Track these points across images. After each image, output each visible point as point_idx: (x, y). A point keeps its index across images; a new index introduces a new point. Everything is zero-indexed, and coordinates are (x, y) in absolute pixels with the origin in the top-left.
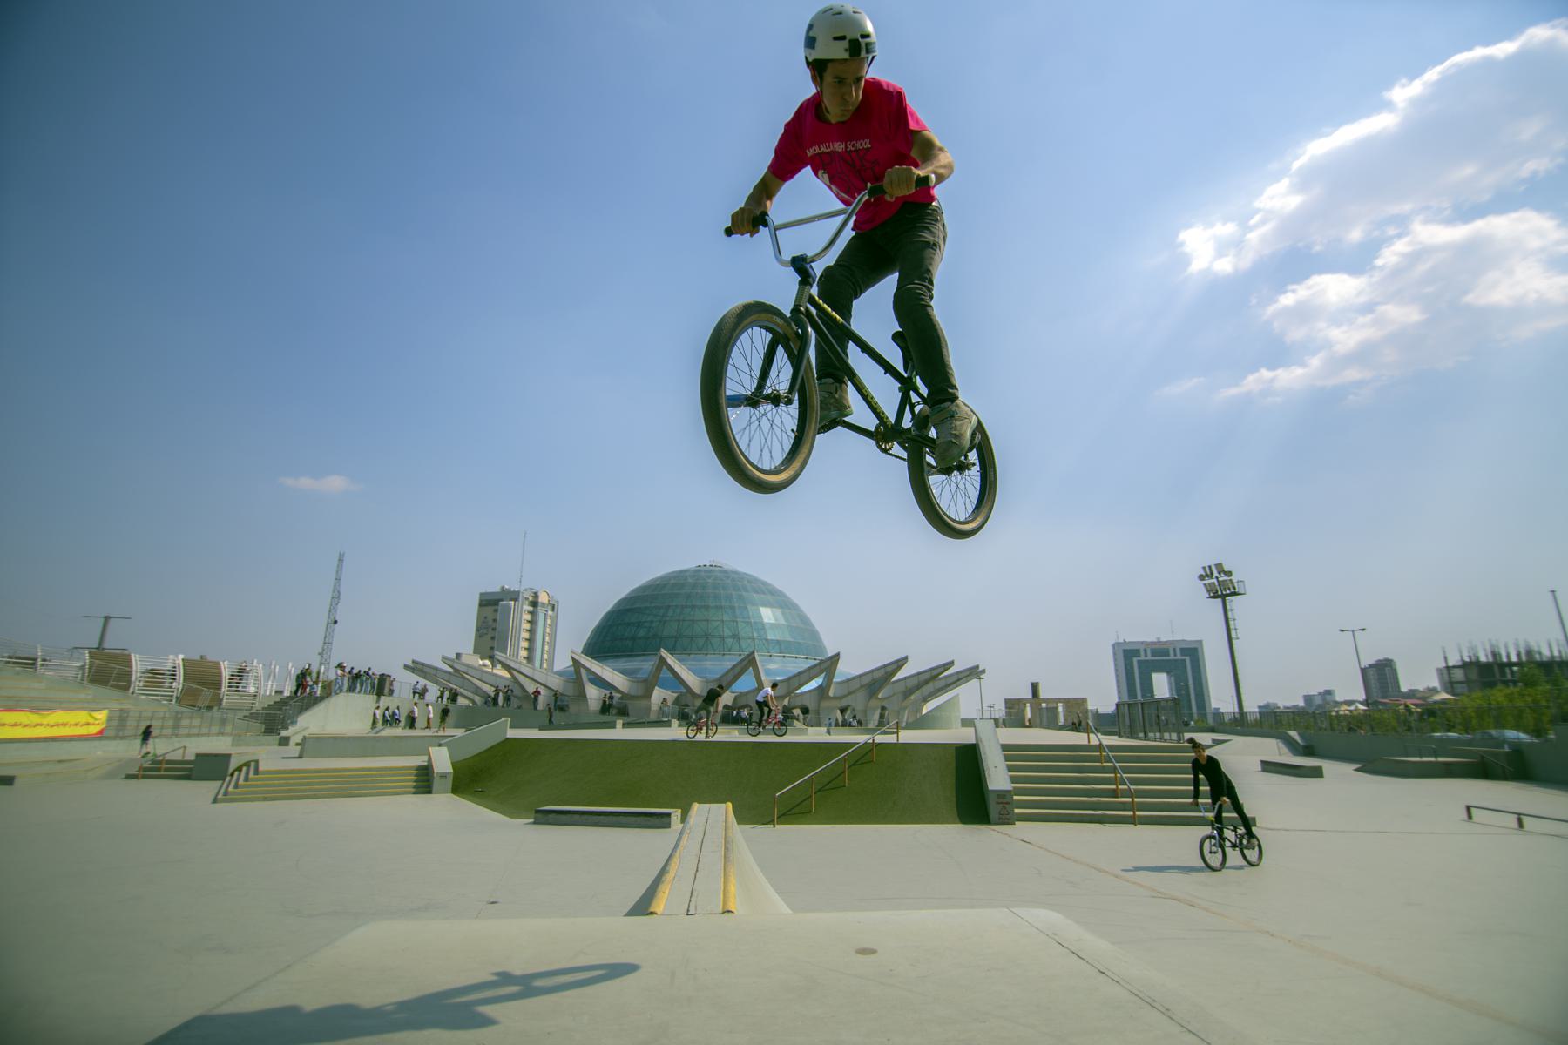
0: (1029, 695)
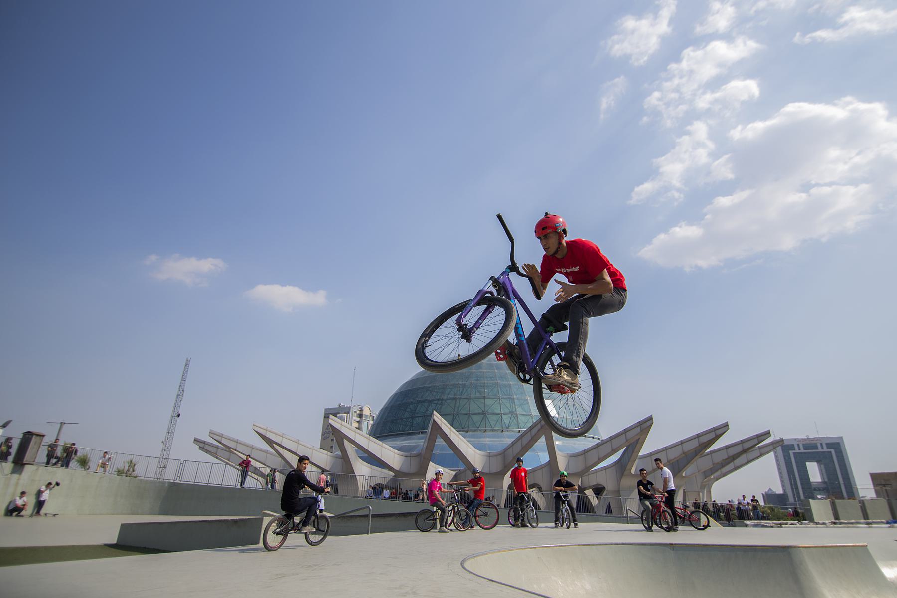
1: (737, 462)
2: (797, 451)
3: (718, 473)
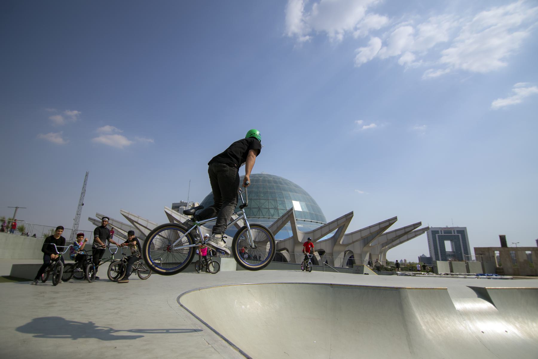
0: (498, 244)
1: (402, 239)
2: (440, 234)
3: (389, 245)
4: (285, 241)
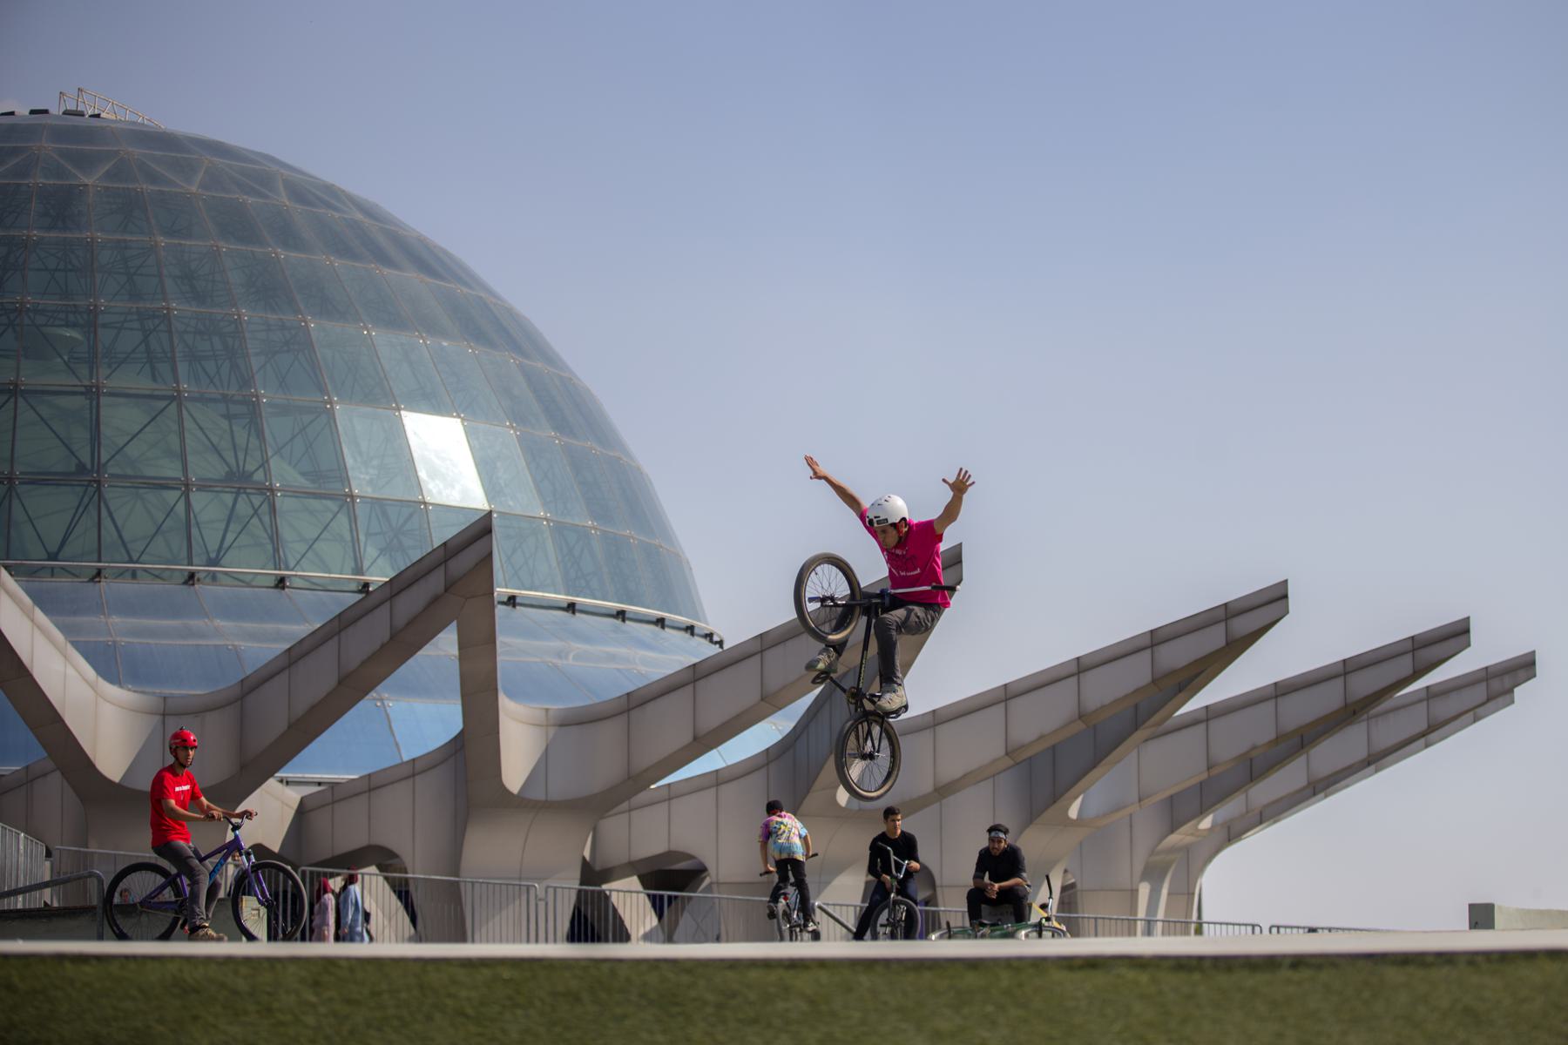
4: (371, 785)
